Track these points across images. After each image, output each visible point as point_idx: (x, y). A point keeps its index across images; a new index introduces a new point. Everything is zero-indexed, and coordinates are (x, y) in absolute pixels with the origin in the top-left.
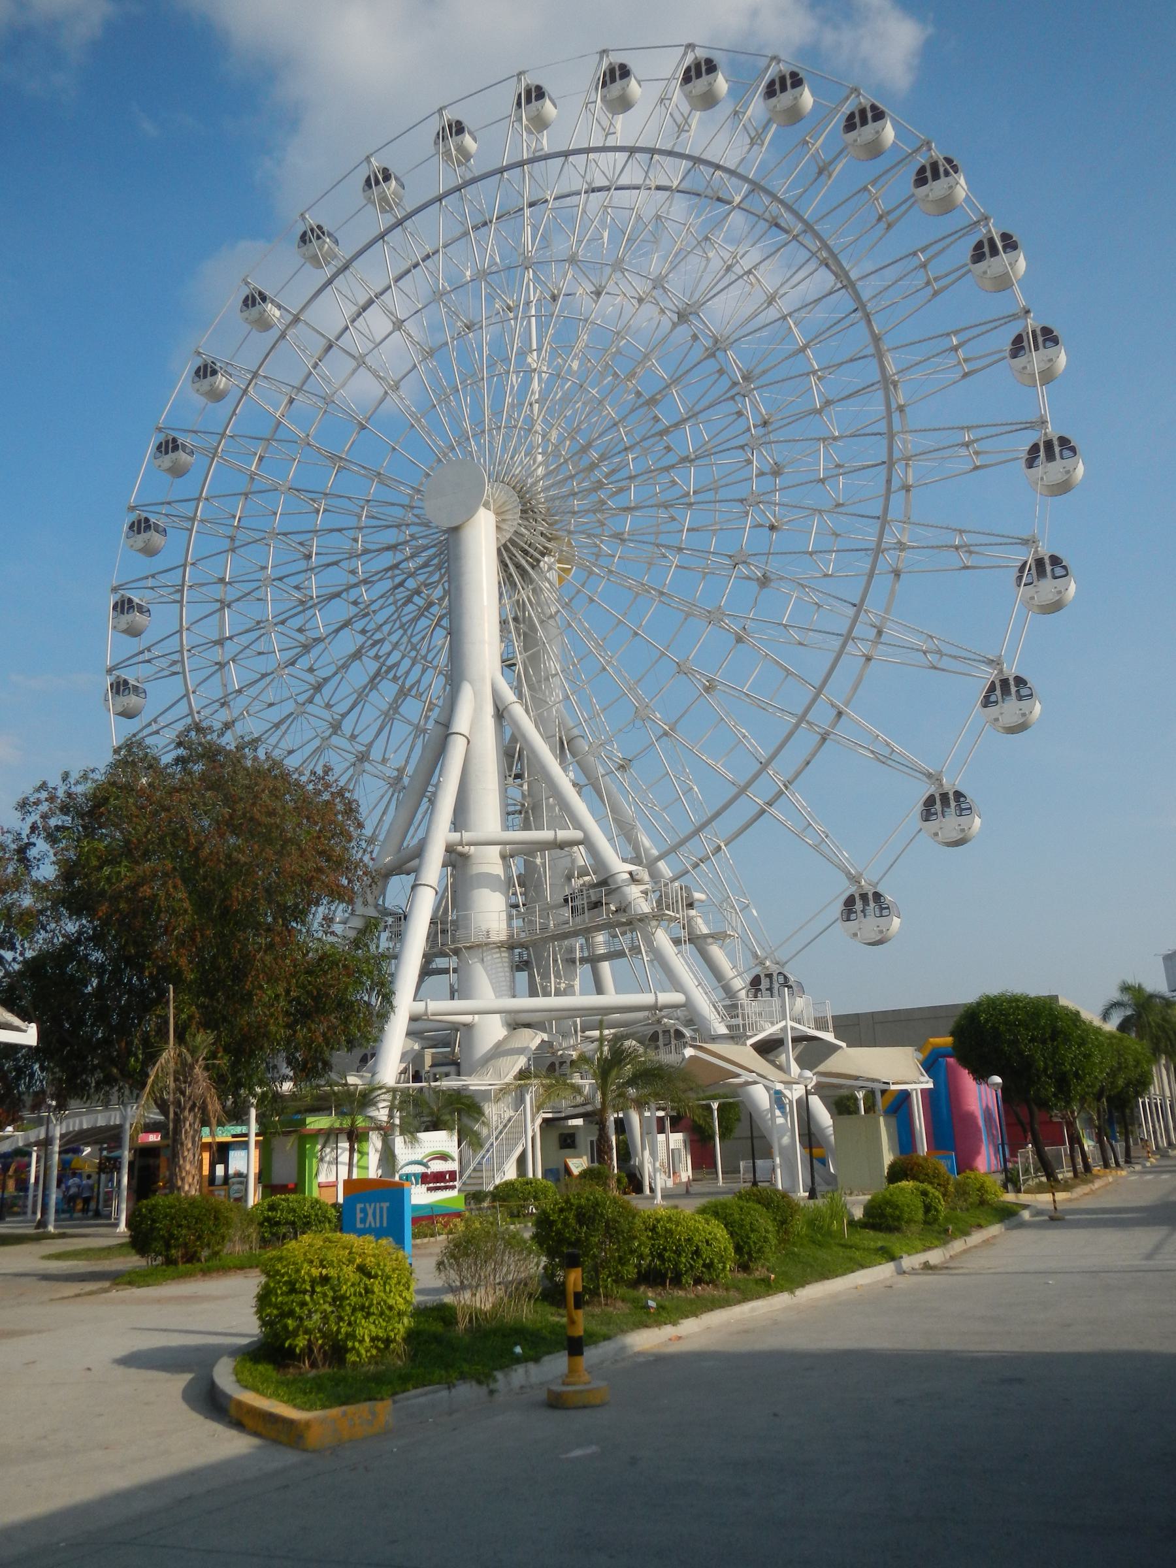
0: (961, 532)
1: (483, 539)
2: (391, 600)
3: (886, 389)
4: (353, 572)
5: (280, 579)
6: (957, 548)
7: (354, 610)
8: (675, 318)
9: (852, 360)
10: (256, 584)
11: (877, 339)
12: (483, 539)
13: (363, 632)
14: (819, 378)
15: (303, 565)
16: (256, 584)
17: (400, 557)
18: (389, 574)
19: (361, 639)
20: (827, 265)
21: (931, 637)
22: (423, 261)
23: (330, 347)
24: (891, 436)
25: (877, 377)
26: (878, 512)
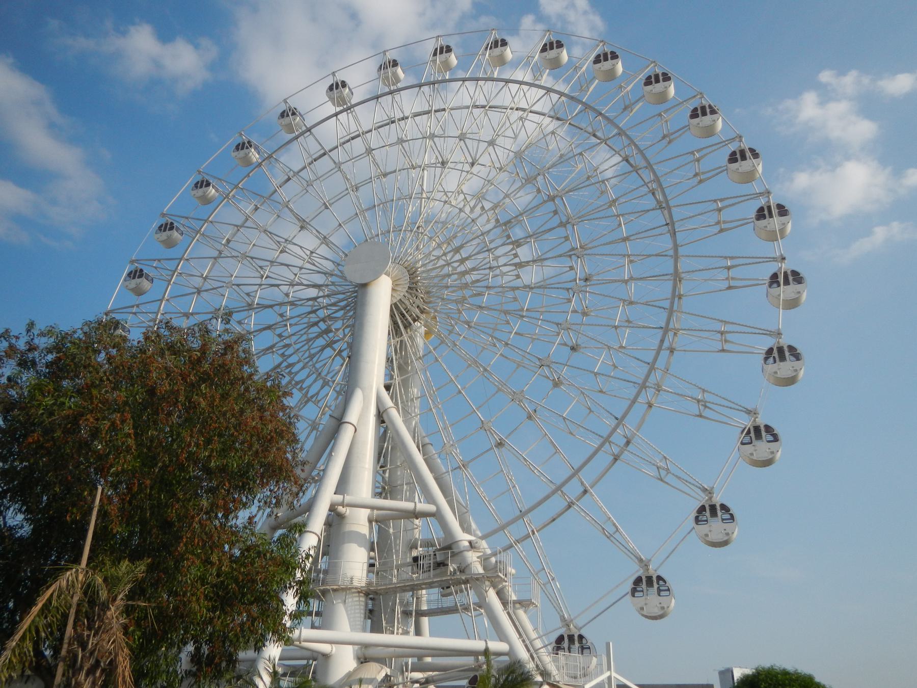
0: (704, 391)
1: (382, 296)
2: (306, 320)
3: (675, 280)
4: (287, 295)
5: (238, 285)
6: (699, 401)
7: (279, 319)
8: (546, 198)
9: (656, 255)
10: (222, 284)
11: (676, 247)
12: (382, 296)
13: (280, 336)
14: (631, 262)
15: (258, 281)
16: (222, 284)
17: (321, 294)
18: (310, 303)
19: (277, 339)
20: (653, 194)
21: (665, 458)
22: (399, 120)
23: (324, 154)
24: (671, 312)
25: (672, 271)
26: (650, 360)
